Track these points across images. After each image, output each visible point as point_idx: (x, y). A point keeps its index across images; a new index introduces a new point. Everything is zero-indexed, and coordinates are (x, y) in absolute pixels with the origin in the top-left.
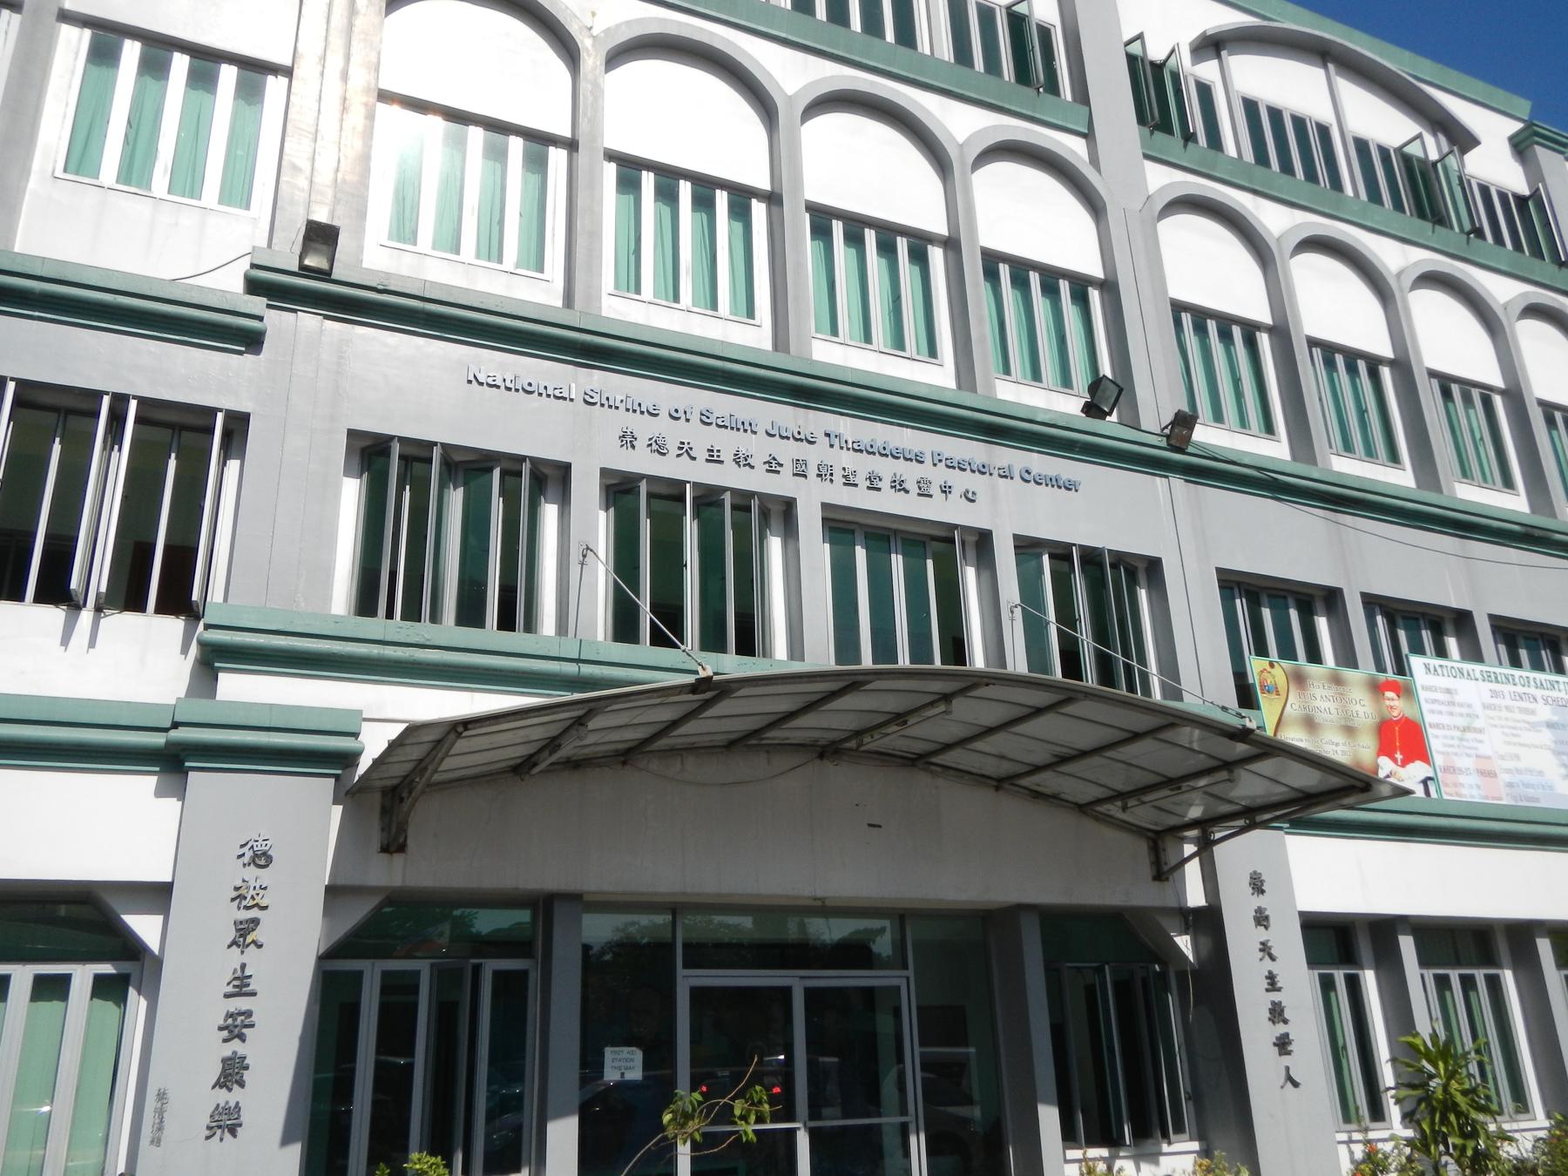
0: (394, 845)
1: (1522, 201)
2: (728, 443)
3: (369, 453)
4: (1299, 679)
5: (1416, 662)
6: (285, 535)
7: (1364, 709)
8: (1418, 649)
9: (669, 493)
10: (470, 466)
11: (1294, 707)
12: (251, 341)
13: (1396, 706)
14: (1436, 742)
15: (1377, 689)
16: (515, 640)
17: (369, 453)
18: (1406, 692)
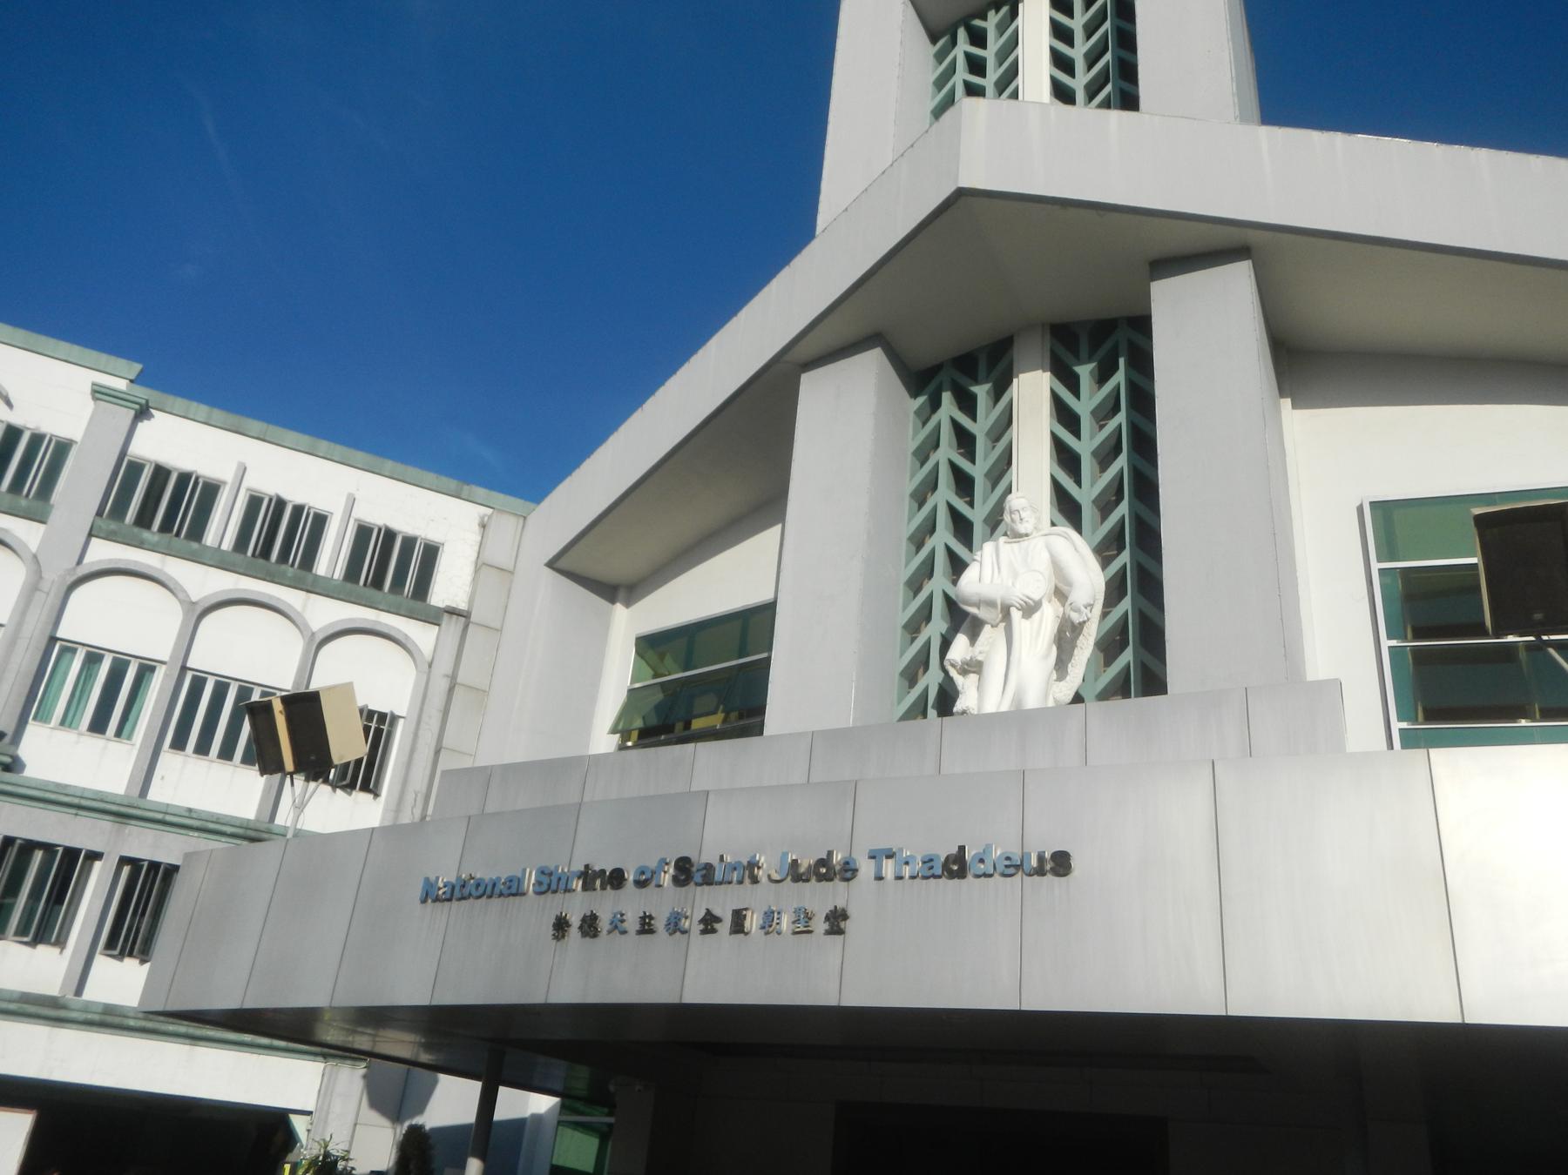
1: (62, 448)
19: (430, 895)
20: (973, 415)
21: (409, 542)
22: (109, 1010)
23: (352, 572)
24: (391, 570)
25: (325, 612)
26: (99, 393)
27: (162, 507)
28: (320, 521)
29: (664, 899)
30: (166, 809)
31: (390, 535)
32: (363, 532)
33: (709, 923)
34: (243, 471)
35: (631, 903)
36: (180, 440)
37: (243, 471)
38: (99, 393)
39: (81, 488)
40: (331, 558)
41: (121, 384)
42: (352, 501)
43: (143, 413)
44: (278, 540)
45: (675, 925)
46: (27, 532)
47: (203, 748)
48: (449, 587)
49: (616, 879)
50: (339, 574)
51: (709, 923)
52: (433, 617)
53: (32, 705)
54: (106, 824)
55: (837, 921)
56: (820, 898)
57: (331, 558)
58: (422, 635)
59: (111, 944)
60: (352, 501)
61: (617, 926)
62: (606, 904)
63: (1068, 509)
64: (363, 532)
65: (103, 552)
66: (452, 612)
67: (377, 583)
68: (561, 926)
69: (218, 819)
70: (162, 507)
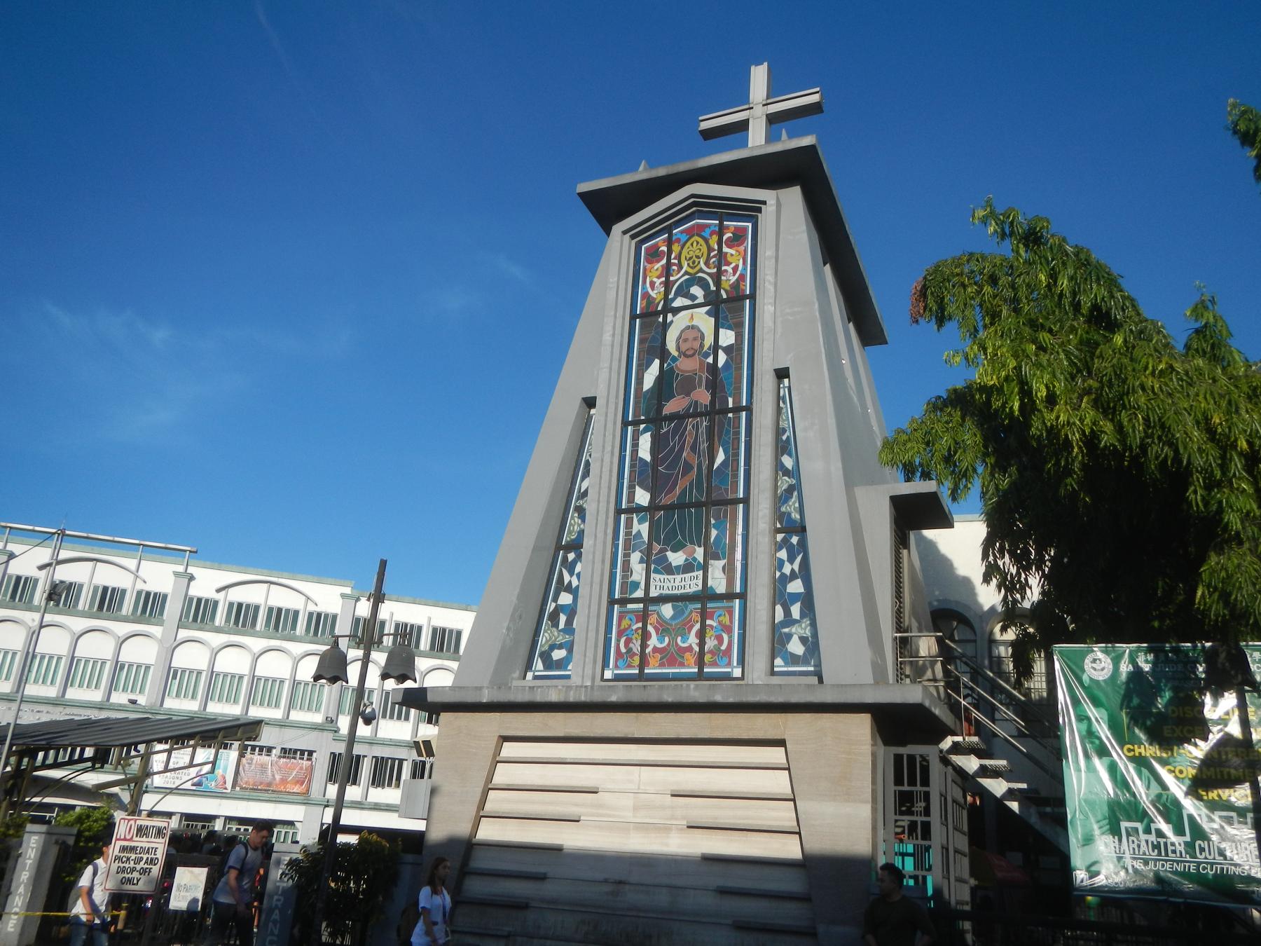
1: (335, 617)
21: (451, 631)
22: (376, 804)
23: (432, 647)
26: (343, 596)
28: (420, 628)
30: (384, 740)
31: (444, 630)
32: (435, 630)
34: (392, 614)
38: (343, 596)
41: (348, 590)
42: (430, 619)
43: (358, 600)
47: (391, 717)
53: (339, 711)
54: (367, 746)
57: (425, 643)
59: (373, 784)
60: (430, 619)
64: (435, 630)
67: (442, 650)
69: (400, 741)
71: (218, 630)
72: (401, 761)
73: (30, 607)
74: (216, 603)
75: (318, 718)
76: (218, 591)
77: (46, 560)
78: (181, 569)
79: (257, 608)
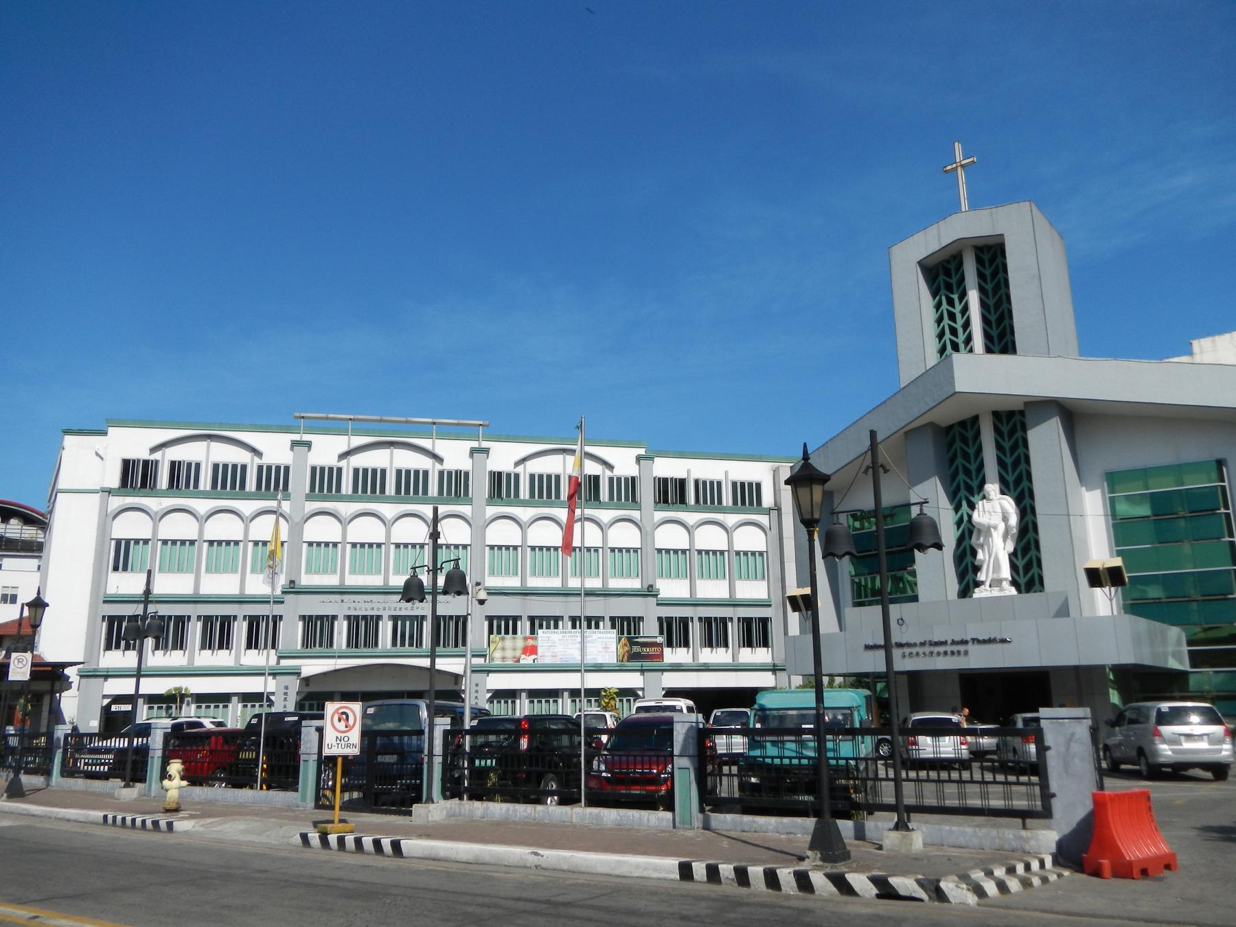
0: (307, 685)
1: (633, 479)
2: (369, 606)
3: (303, 618)
4: (503, 639)
5: (540, 631)
6: (292, 633)
7: (520, 643)
8: (541, 627)
9: (356, 617)
10: (321, 618)
11: (500, 645)
12: (282, 602)
13: (530, 642)
14: (540, 651)
15: (526, 639)
16: (329, 650)
17: (303, 618)
18: (536, 639)
19: (868, 647)
20: (968, 446)
21: (750, 484)
24: (747, 495)
25: (731, 519)
27: (671, 493)
28: (719, 483)
29: (927, 649)
32: (734, 484)
33: (939, 654)
34: (689, 471)
35: (921, 650)
36: (668, 468)
37: (689, 471)
39: (647, 493)
40: (727, 499)
41: (642, 451)
42: (726, 473)
44: (708, 494)
45: (931, 653)
46: (636, 514)
48: (767, 499)
49: (915, 645)
50: (730, 503)
51: (939, 654)
52: (768, 511)
55: (966, 653)
56: (962, 648)
57: (727, 499)
58: (763, 519)
60: (726, 473)
61: (917, 654)
62: (914, 650)
63: (1003, 482)
64: (734, 484)
65: (659, 515)
66: (770, 509)
67: (743, 503)
68: (904, 656)
70: (671, 493)
71: (524, 504)
72: (724, 621)
73: (341, 498)
74: (517, 476)
75: (635, 584)
76: (517, 464)
77: (345, 449)
78: (475, 444)
79: (558, 477)
